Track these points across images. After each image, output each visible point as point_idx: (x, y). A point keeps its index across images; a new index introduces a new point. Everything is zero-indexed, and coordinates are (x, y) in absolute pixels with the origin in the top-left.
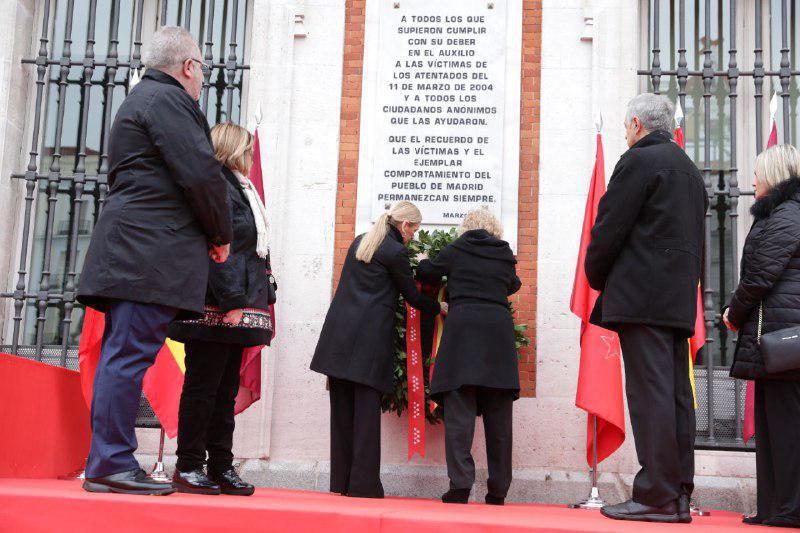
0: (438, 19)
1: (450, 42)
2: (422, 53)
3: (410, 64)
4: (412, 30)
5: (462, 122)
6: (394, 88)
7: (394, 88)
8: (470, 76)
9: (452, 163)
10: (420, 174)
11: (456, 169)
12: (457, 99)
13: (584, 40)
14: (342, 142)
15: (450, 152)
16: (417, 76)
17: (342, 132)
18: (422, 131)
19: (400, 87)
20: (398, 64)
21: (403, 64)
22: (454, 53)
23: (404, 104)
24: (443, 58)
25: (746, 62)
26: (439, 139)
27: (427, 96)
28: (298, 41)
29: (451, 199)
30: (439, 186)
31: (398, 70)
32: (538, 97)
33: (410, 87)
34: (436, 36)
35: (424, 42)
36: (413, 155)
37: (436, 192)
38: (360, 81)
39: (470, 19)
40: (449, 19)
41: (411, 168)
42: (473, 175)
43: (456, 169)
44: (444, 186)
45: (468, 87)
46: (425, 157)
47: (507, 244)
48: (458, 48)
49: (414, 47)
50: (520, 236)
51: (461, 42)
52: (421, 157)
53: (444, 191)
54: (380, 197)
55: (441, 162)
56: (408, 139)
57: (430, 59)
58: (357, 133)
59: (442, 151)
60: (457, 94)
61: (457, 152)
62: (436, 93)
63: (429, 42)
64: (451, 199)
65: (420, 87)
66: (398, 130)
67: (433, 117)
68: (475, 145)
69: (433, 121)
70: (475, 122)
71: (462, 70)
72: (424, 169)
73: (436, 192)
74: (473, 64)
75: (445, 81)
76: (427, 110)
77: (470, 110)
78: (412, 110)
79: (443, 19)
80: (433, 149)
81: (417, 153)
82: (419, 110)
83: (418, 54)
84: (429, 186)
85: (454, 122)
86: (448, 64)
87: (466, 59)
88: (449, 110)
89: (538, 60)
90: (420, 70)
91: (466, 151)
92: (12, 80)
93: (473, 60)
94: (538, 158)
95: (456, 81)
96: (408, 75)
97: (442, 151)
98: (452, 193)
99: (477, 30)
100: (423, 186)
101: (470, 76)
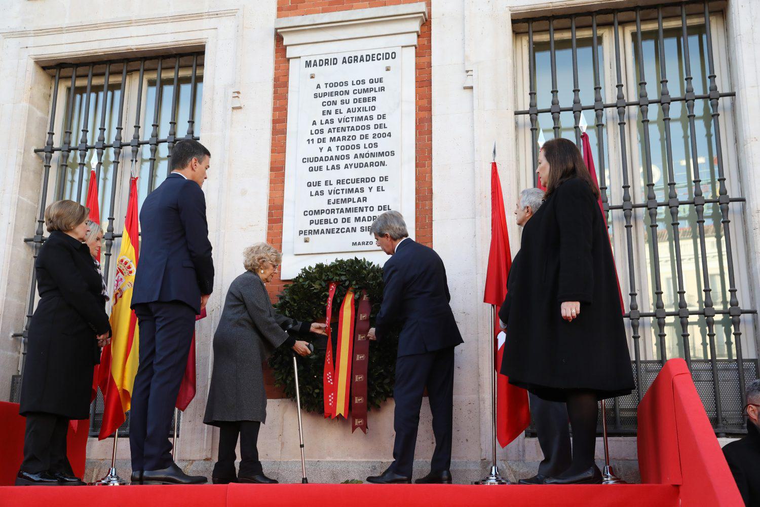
0: (346, 83)
2: (333, 112)
3: (324, 122)
4: (325, 94)
5: (366, 165)
6: (311, 142)
7: (311, 142)
8: (372, 127)
9: (359, 200)
10: (333, 211)
12: (362, 146)
13: (465, 88)
14: (272, 189)
15: (357, 191)
16: (330, 131)
17: (271, 182)
18: (334, 176)
19: (316, 141)
20: (314, 123)
21: (318, 122)
23: (319, 155)
24: (350, 115)
26: (347, 181)
27: (338, 147)
28: (235, 111)
29: (358, 229)
30: (348, 220)
31: (314, 128)
32: (430, 139)
33: (324, 140)
34: (345, 97)
35: (335, 103)
36: (327, 196)
37: (346, 225)
39: (371, 81)
40: (355, 83)
41: (326, 207)
42: (376, 208)
44: (352, 220)
45: (370, 136)
46: (336, 197)
48: (362, 105)
49: (327, 108)
51: (365, 100)
52: (333, 197)
53: (352, 224)
55: (349, 200)
56: (323, 183)
57: (340, 116)
58: (283, 182)
59: (350, 191)
60: (362, 143)
61: (362, 190)
62: (345, 143)
63: (339, 103)
64: (358, 229)
65: (332, 139)
66: (315, 177)
67: (342, 163)
68: (377, 183)
69: (342, 166)
70: (378, 164)
71: (365, 123)
72: (336, 206)
73: (346, 225)
74: (375, 117)
75: (352, 133)
76: (337, 158)
77: (373, 155)
78: (327, 159)
79: (350, 83)
80: (343, 190)
81: (330, 194)
82: (332, 158)
84: (340, 221)
85: (360, 165)
86: (354, 119)
87: (368, 114)
88: (356, 156)
89: (430, 110)
90: (331, 126)
91: (370, 189)
92: (23, 166)
93: (375, 114)
95: (361, 132)
96: (322, 131)
97: (350, 191)
98: (358, 225)
99: (377, 90)
100: (336, 221)
101: (372, 127)
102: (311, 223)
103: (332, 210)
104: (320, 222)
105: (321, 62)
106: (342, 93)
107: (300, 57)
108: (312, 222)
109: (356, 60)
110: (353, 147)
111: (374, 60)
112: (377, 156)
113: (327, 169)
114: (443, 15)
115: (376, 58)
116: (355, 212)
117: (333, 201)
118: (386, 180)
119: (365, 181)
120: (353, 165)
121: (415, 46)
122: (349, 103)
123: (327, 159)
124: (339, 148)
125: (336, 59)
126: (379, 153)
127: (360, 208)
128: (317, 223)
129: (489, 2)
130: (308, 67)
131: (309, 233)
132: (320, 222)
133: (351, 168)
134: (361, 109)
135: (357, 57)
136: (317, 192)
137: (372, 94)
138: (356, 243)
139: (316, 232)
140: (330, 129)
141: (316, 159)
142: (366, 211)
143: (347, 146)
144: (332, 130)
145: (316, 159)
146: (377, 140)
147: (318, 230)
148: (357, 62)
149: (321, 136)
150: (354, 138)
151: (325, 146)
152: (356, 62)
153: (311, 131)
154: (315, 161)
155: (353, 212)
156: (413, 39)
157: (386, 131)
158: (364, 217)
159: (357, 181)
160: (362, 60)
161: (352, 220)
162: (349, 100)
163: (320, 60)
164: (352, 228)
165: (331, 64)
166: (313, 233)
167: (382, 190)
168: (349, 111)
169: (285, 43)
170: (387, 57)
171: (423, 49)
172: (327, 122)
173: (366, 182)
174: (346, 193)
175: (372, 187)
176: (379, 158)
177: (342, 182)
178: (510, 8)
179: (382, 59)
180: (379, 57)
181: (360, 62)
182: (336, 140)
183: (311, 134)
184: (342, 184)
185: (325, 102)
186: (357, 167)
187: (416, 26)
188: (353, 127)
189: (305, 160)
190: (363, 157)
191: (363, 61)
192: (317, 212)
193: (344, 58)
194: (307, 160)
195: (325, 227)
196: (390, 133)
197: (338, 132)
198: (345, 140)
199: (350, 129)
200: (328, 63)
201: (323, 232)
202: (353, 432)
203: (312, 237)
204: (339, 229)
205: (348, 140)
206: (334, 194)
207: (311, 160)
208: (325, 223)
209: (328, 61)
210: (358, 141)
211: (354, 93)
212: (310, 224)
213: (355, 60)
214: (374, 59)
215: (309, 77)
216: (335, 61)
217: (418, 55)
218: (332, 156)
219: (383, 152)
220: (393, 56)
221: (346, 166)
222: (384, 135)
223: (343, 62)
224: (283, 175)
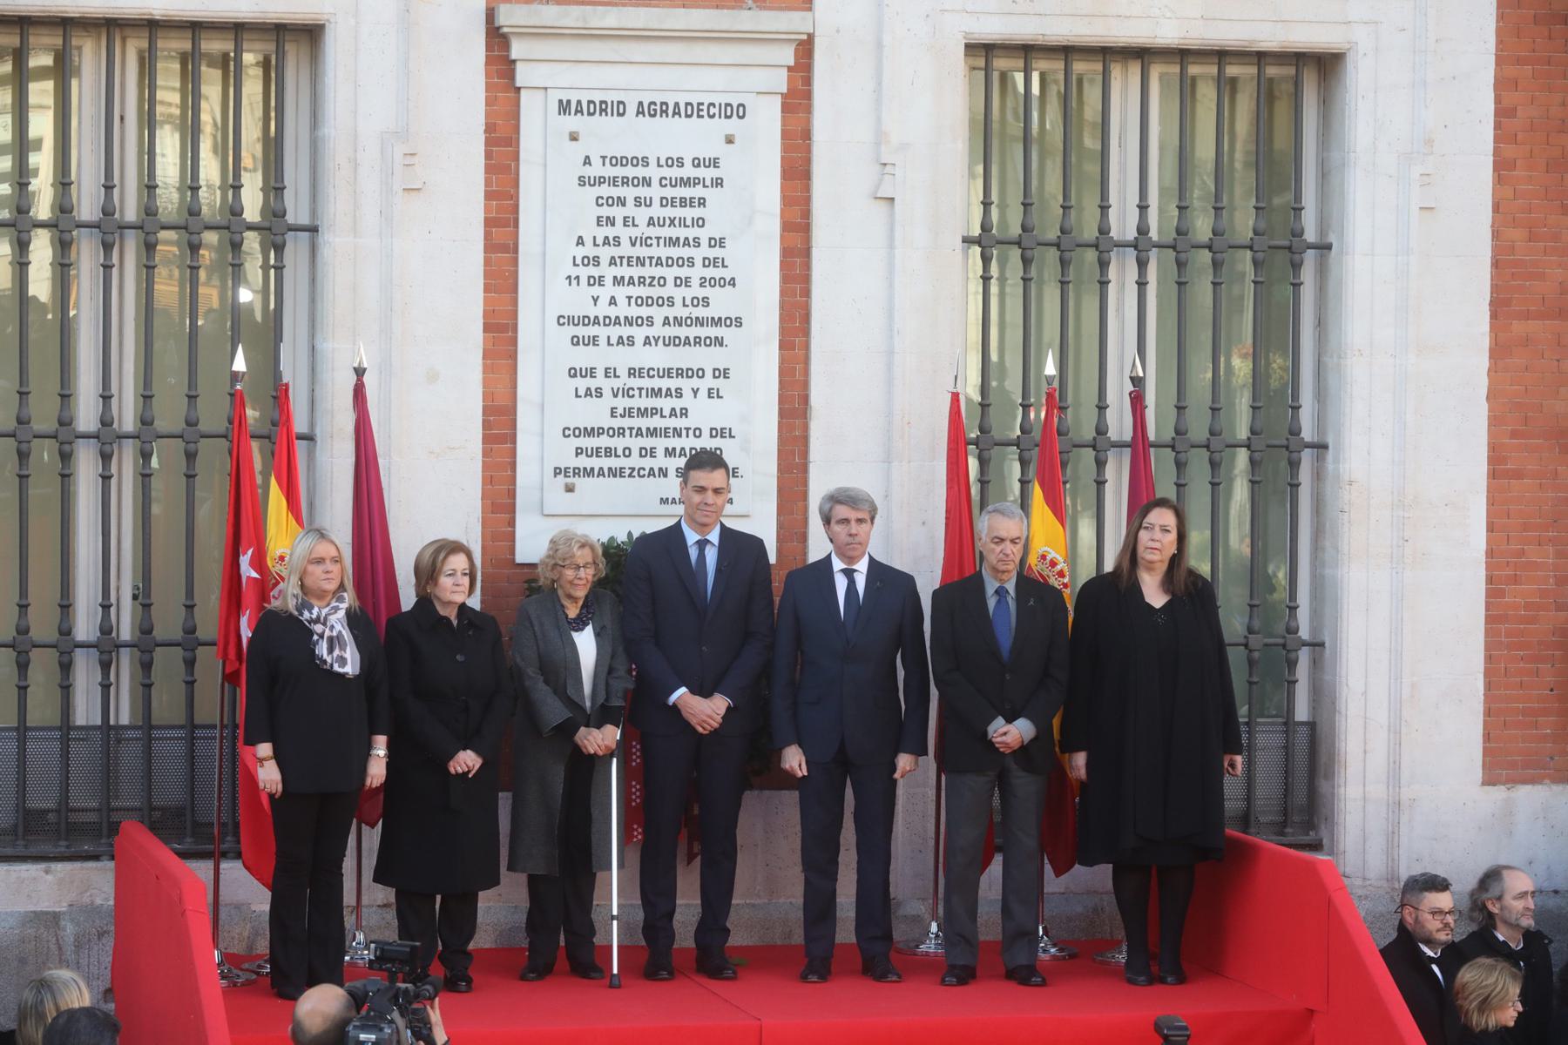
0: (645, 162)
1: (666, 202)
2: (619, 222)
3: (600, 241)
4: (601, 180)
5: (687, 342)
7: (574, 282)
8: (698, 262)
9: (673, 413)
10: (621, 432)
12: (678, 302)
14: (487, 369)
15: (669, 393)
16: (612, 262)
17: (486, 355)
18: (623, 358)
19: (584, 281)
20: (580, 241)
21: (588, 241)
23: (592, 312)
24: (654, 232)
25: (1123, 224)
26: (649, 373)
27: (629, 298)
31: (580, 252)
34: (642, 192)
35: (622, 202)
36: (608, 401)
37: (647, 463)
38: (515, 262)
39: (697, 163)
40: (663, 162)
41: (607, 422)
42: (706, 433)
44: (660, 452)
45: (695, 282)
48: (678, 212)
49: (606, 211)
50: (781, 526)
51: (684, 202)
52: (622, 403)
53: (661, 461)
54: (557, 471)
55: (654, 412)
56: (600, 373)
58: (513, 356)
59: (656, 393)
60: (679, 294)
62: (643, 291)
63: (630, 202)
65: (618, 281)
66: (584, 357)
67: (639, 333)
68: (709, 381)
69: (639, 340)
72: (626, 423)
73: (647, 463)
74: (704, 242)
75: (658, 272)
76: (629, 321)
77: (699, 322)
78: (609, 321)
79: (653, 162)
80: (640, 389)
81: (615, 396)
82: (617, 321)
83: (613, 225)
84: (635, 453)
85: (674, 342)
86: (662, 241)
87: (691, 233)
88: (666, 322)
91: (695, 392)
93: (703, 234)
94: (805, 399)
96: (596, 261)
97: (656, 393)
99: (708, 183)
100: (627, 452)
101: (698, 262)
102: (577, 454)
103: (619, 429)
104: (596, 452)
105: (592, 106)
106: (636, 182)
107: (546, 88)
108: (579, 451)
109: (664, 112)
110: (660, 302)
111: (702, 117)
112: (707, 326)
113: (609, 344)
114: (838, 31)
115: (704, 113)
116: (666, 436)
117: (620, 411)
118: (725, 377)
119: (685, 374)
120: (661, 339)
121: (782, 94)
122: (650, 205)
123: (607, 321)
124: (633, 301)
125: (623, 103)
126: (713, 318)
127: (675, 429)
128: (589, 453)
129: (927, 16)
130: (565, 114)
131: (574, 474)
132: (596, 452)
133: (656, 345)
134: (677, 222)
135: (666, 104)
136: (589, 389)
137: (698, 192)
138: (667, 499)
139: (589, 472)
140: (613, 258)
141: (586, 321)
142: (687, 436)
143: (647, 298)
144: (618, 261)
145: (586, 321)
146: (707, 291)
147: (592, 469)
148: (667, 116)
149: (595, 272)
150: (662, 282)
151: (605, 292)
152: (664, 115)
153: (574, 257)
154: (584, 325)
155: (661, 436)
156: (780, 81)
157: (727, 274)
158: (683, 449)
159: (669, 373)
160: (677, 113)
161: (660, 452)
162: (651, 198)
163: (590, 102)
164: (660, 469)
165: (612, 115)
166: (582, 474)
167: (718, 397)
168: (651, 222)
169: (514, 55)
170: (729, 114)
172: (606, 241)
173: (687, 376)
174: (647, 396)
175: (698, 389)
177: (640, 373)
179: (717, 115)
180: (712, 111)
181: (673, 116)
182: (626, 283)
183: (575, 265)
184: (640, 377)
185: (602, 198)
186: (669, 345)
187: (787, 56)
188: (659, 258)
189: (562, 321)
190: (680, 325)
191: (680, 116)
192: (589, 432)
193: (641, 104)
194: (566, 321)
196: (733, 279)
197: (629, 265)
198: (645, 285)
199: (654, 261)
200: (605, 110)
201: (601, 473)
202: (689, 863)
203: (581, 483)
204: (633, 469)
205: (650, 285)
206: (623, 396)
207: (576, 322)
208: (606, 456)
209: (607, 107)
210: (669, 290)
211: (661, 185)
212: (577, 456)
213: (662, 111)
214: (701, 113)
215: (567, 137)
216: (620, 109)
217: (786, 108)
218: (617, 317)
219: (720, 319)
220: (740, 111)
221: (647, 341)
222: (722, 281)
223: (638, 113)
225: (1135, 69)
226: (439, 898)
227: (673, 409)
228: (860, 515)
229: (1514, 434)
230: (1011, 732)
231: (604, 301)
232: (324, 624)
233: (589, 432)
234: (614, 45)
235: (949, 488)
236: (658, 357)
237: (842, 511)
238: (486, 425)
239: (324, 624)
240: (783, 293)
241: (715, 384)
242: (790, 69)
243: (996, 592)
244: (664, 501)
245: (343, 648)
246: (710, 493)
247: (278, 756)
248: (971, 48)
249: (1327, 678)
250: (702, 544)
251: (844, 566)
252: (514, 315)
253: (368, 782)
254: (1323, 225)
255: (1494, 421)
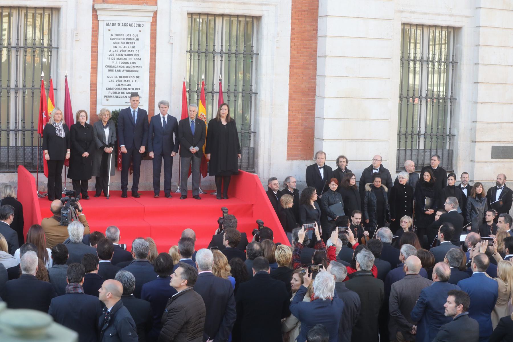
1: (127, 43)
2: (118, 47)
3: (114, 51)
4: (115, 39)
5: (131, 71)
8: (134, 55)
9: (128, 85)
10: (118, 89)
11: (129, 87)
12: (129, 63)
14: (91, 76)
15: (127, 81)
16: (117, 55)
18: (118, 74)
19: (111, 59)
20: (110, 51)
21: (112, 51)
22: (128, 47)
24: (125, 49)
25: (218, 49)
31: (110, 53)
34: (123, 41)
36: (115, 82)
37: (123, 95)
38: (97, 55)
39: (134, 35)
40: (127, 35)
41: (115, 87)
42: (135, 89)
43: (129, 87)
44: (125, 93)
45: (133, 59)
46: (119, 83)
47: (146, 111)
49: (115, 45)
51: (131, 43)
52: (118, 83)
53: (125, 95)
54: (105, 96)
55: (124, 85)
59: (125, 81)
60: (130, 61)
62: (123, 61)
63: (120, 43)
65: (118, 59)
66: (111, 74)
67: (122, 69)
68: (135, 79)
69: (122, 71)
71: (131, 53)
72: (119, 87)
73: (123, 95)
74: (135, 51)
75: (125, 57)
76: (120, 67)
77: (134, 67)
78: (115, 67)
79: (125, 35)
80: (122, 80)
81: (117, 81)
82: (117, 67)
84: (120, 93)
85: (128, 71)
87: (132, 49)
88: (127, 67)
91: (133, 81)
93: (135, 49)
94: (154, 83)
95: (129, 57)
96: (113, 55)
97: (125, 81)
100: (119, 93)
101: (134, 55)
110: (126, 63)
117: (118, 85)
137: (134, 41)
139: (111, 97)
149: (113, 57)
156: (150, 20)
160: (130, 26)
161: (125, 93)
168: (124, 47)
169: (98, 14)
171: (154, 23)
172: (115, 51)
176: (136, 68)
178: (187, 11)
180: (137, 25)
187: (152, 15)
192: (111, 89)
193: (123, 24)
195: (115, 95)
201: (114, 97)
203: (109, 99)
216: (119, 25)
217: (152, 25)
220: (142, 25)
221: (123, 71)
223: (122, 25)
224: (97, 70)
225: (221, 18)
226: (80, 181)
227: (128, 84)
228: (165, 106)
229: (294, 92)
230: (194, 149)
231: (115, 63)
232: (58, 127)
233: (111, 89)
234: (118, 12)
235: (183, 101)
236: (126, 74)
237: (162, 105)
238: (91, 87)
239: (58, 127)
240: (150, 62)
241: (136, 79)
242: (152, 17)
243: (192, 121)
244: (126, 103)
245: (62, 132)
246: (136, 101)
247: (49, 153)
248: (188, 14)
249: (257, 139)
250: (134, 111)
251: (163, 116)
252: (97, 65)
253: (66, 158)
254: (257, 50)
255: (290, 89)
